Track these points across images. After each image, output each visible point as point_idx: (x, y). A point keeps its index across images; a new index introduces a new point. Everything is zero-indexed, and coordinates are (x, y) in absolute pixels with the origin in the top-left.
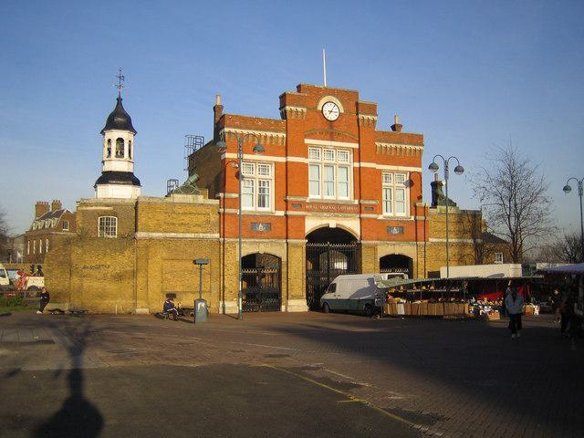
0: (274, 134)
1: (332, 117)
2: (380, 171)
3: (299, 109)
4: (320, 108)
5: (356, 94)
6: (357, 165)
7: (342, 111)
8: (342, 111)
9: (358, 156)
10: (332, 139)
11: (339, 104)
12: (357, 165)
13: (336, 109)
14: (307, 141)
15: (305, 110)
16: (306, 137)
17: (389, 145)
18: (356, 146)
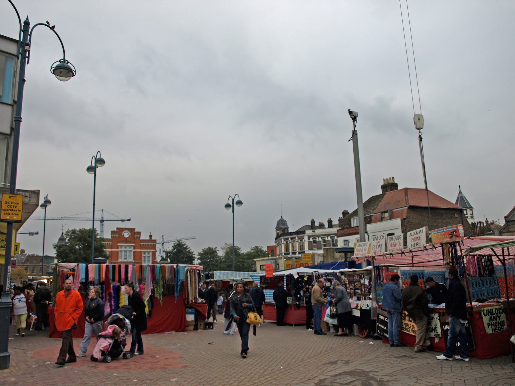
0: (108, 243)
1: (127, 236)
2: (142, 251)
3: (116, 235)
4: (123, 234)
5: (135, 229)
6: (134, 250)
7: (130, 234)
8: (130, 234)
9: (135, 248)
10: (126, 243)
11: (129, 232)
12: (134, 250)
13: (127, 234)
14: (118, 244)
15: (118, 235)
16: (118, 243)
17: (145, 244)
18: (134, 244)
